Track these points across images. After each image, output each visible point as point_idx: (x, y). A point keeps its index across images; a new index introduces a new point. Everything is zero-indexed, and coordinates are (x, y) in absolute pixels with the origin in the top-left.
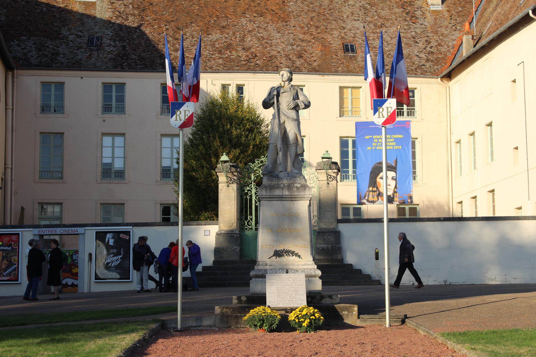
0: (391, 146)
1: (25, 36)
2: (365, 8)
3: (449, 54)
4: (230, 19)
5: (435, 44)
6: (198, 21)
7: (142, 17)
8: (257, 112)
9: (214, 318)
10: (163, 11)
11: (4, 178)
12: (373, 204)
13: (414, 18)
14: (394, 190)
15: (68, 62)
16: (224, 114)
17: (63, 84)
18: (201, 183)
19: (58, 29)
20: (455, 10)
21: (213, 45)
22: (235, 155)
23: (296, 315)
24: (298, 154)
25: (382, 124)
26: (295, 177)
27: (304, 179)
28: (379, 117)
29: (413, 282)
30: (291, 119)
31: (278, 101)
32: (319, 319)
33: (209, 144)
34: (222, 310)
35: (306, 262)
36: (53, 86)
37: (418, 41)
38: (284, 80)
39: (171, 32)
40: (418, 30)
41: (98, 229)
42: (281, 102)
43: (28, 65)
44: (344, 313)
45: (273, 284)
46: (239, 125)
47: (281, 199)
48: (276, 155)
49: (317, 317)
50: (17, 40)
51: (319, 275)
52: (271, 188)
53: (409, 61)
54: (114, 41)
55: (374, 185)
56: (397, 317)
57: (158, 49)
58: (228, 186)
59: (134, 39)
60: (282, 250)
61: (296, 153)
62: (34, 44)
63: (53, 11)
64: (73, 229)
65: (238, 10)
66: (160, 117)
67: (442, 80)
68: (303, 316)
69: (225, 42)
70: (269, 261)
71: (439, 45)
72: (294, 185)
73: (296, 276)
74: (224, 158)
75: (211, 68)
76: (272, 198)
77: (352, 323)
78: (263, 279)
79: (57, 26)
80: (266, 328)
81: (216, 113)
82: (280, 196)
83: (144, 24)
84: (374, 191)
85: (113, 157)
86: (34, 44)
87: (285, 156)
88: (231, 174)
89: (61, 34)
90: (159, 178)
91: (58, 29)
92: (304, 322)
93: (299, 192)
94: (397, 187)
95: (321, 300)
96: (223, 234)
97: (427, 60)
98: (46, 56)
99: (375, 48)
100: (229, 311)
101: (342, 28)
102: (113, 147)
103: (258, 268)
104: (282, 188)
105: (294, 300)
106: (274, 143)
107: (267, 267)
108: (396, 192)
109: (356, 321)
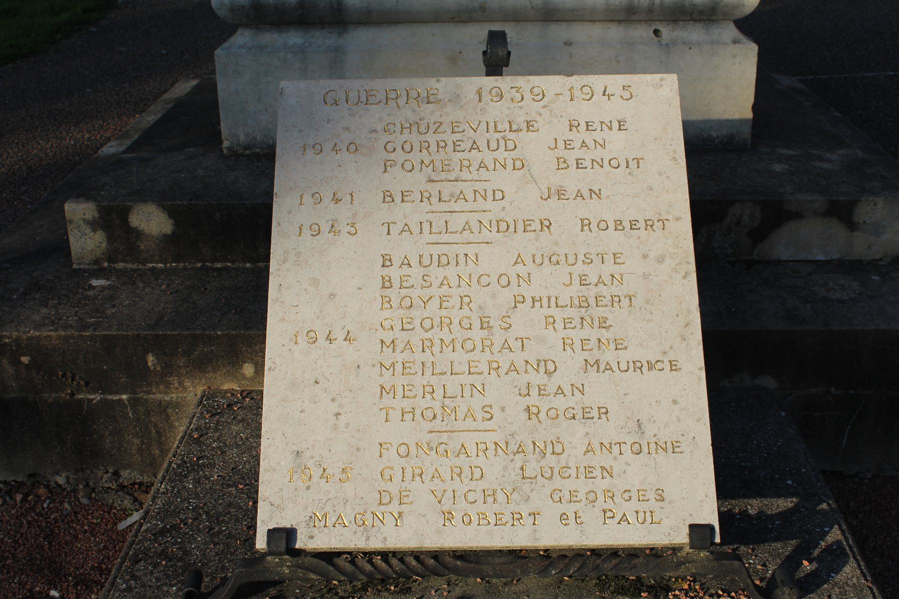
73: (584, 111)
95: (760, 234)
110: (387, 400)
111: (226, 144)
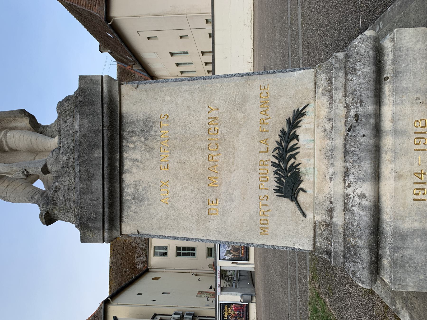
1: (135, 261)
11: (195, 274)
17: (155, 247)
19: (132, 247)
35: (320, 91)
43: (147, 262)
47: (117, 173)
50: (136, 265)
60: (276, 173)
61: (30, 130)
62: (138, 258)
64: (217, 273)
86: (138, 258)
89: (134, 246)
91: (132, 247)
98: (143, 253)
103: (342, 254)
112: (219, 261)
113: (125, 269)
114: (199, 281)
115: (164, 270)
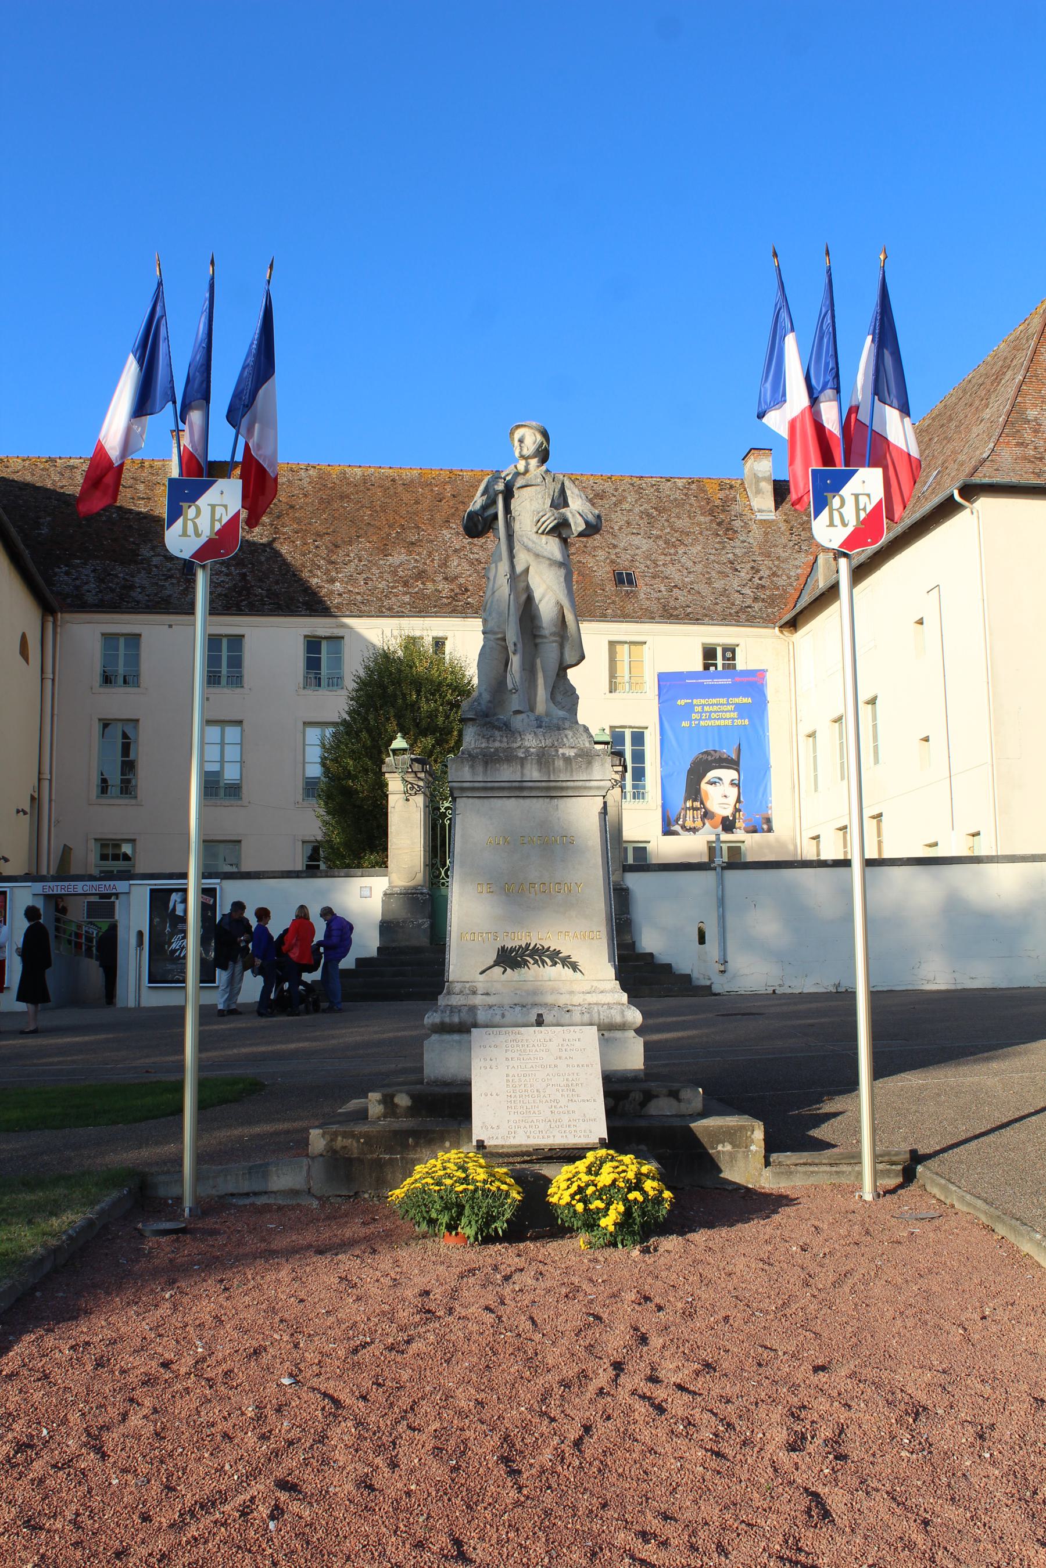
0: (728, 719)
2: (649, 515)
3: (790, 590)
4: (423, 530)
5: (768, 573)
6: (369, 535)
7: (276, 528)
8: (467, 673)
9: (305, 1168)
10: (311, 518)
11: (36, 796)
12: (695, 833)
13: (730, 531)
14: (735, 806)
15: (148, 601)
16: (407, 676)
18: (363, 800)
19: (134, 547)
20: (796, 520)
21: (394, 573)
22: (425, 747)
23: (574, 1188)
24: (565, 665)
25: (841, 546)
26: (559, 729)
27: (585, 735)
28: (832, 524)
29: (774, 988)
30: (547, 562)
31: (507, 510)
32: (658, 1200)
33: (378, 729)
34: (332, 1140)
35: (595, 984)
36: (122, 640)
37: (738, 567)
38: (525, 452)
39: (323, 552)
40: (737, 551)
41: (155, 885)
42: (517, 513)
43: (80, 605)
44: (720, 1148)
45: (494, 1063)
46: (433, 694)
48: (503, 667)
49: (651, 1193)
51: (634, 1023)
52: (489, 759)
53: (726, 600)
54: (228, 567)
55: (696, 797)
56: (886, 1158)
57: (302, 580)
58: (407, 800)
59: (261, 563)
60: (520, 947)
62: (94, 571)
63: (128, 519)
64: (107, 883)
65: (438, 516)
66: (302, 692)
67: (781, 632)
68: (600, 1193)
69: (415, 567)
70: (481, 982)
71: (774, 574)
72: (557, 751)
74: (399, 743)
75: (390, 609)
76: (492, 789)
77: (748, 1182)
78: (465, 1036)
79: (134, 543)
80: (470, 1232)
81: (391, 674)
82: (514, 784)
83: (279, 538)
84: (697, 809)
85: (222, 762)
86: (94, 571)
87: (529, 670)
88: (413, 775)
89: (139, 555)
90: (300, 798)
92: (606, 1212)
93: (572, 771)
94: (742, 799)
95: (643, 1104)
96: (397, 894)
97: (756, 599)
98: (112, 590)
99: (667, 578)
100: (355, 1144)
101: (611, 546)
102: (222, 744)
103: (450, 1003)
104: (522, 761)
105: (565, 1118)
106: (496, 629)
107: (478, 1000)
108: (739, 811)
109: (760, 1175)
110: (510, 1110)
111: (425, 1080)
112: (148, 888)
113: (48, 519)
114: (18, 811)
115: (49, 675)
